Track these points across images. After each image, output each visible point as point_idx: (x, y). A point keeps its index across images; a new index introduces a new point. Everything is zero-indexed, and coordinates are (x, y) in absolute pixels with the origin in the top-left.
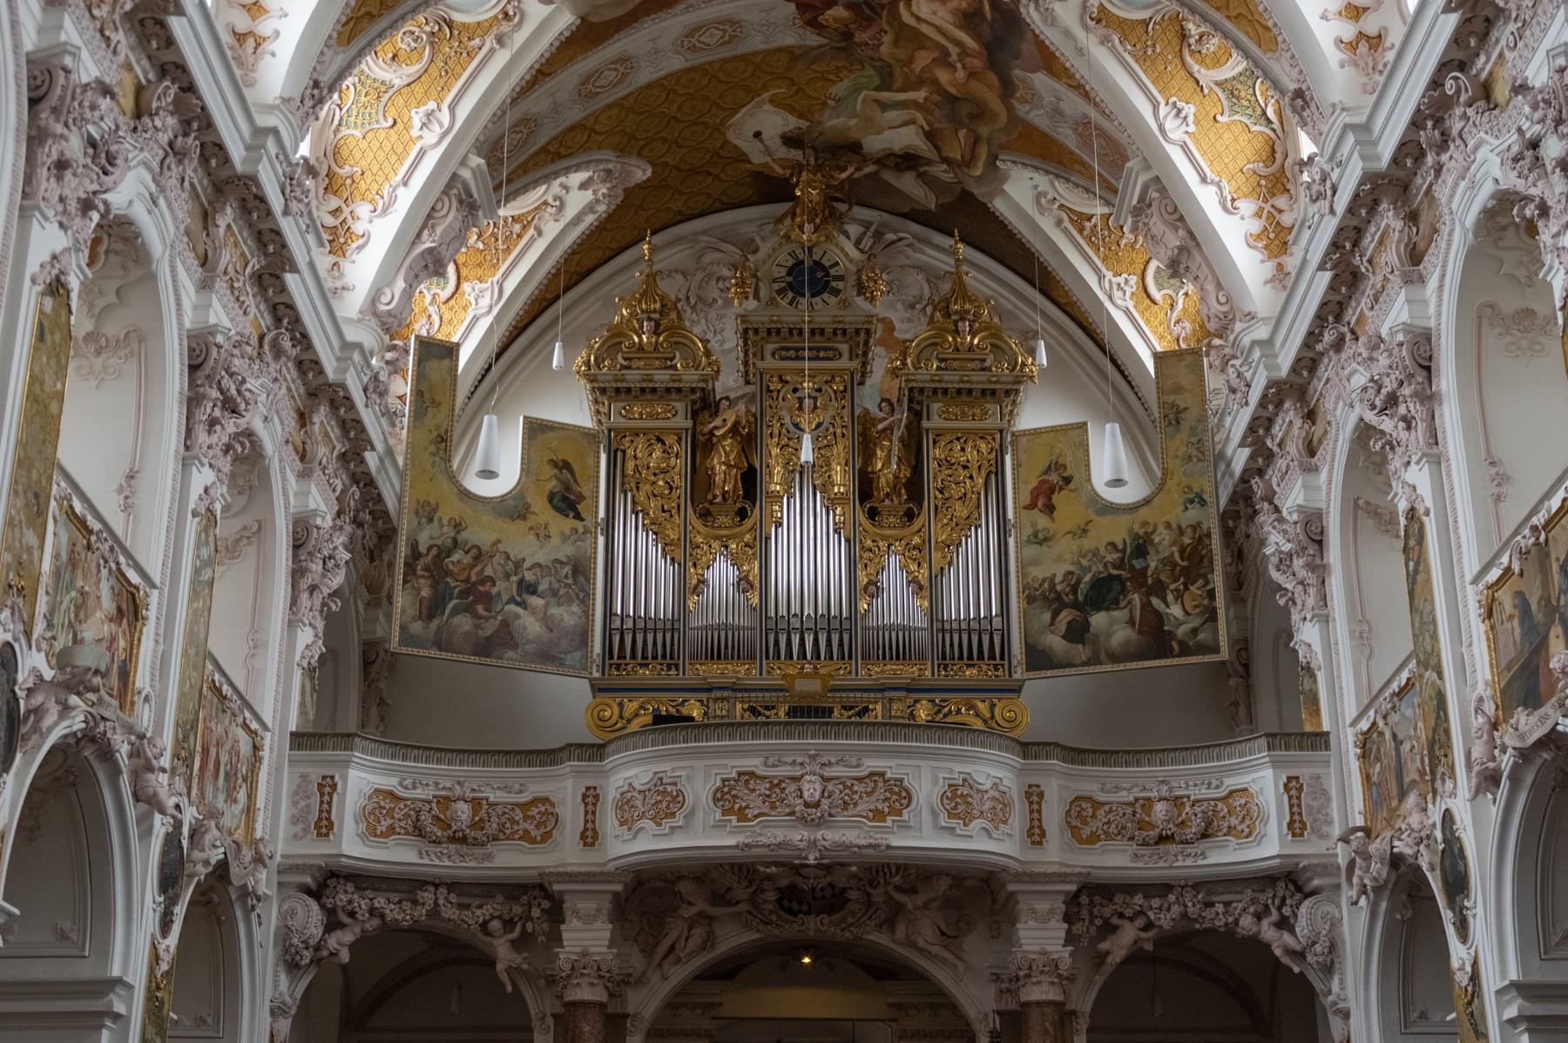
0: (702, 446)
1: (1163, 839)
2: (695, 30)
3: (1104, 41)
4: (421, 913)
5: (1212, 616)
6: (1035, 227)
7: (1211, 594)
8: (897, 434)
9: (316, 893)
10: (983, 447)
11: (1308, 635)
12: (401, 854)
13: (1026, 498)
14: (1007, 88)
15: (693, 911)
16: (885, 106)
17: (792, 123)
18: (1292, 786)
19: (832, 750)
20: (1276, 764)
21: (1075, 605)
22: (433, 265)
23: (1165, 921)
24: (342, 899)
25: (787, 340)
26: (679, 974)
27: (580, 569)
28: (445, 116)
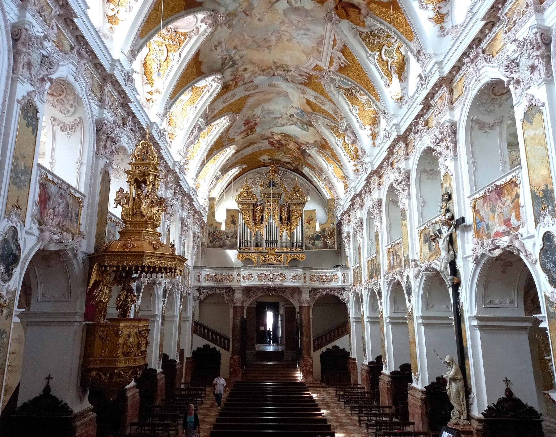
0: (255, 212)
1: (324, 282)
2: (253, 148)
3: (319, 155)
4: (213, 292)
5: (335, 243)
6: (309, 174)
7: (334, 239)
8: (286, 210)
9: (198, 290)
10: (299, 213)
11: (347, 250)
12: (210, 284)
13: (306, 222)
14: (304, 158)
15: (253, 292)
16: (285, 156)
17: (269, 157)
18: (343, 275)
19: (274, 270)
20: (341, 271)
21: (313, 239)
22: (213, 188)
23: (324, 293)
24: (202, 290)
25: (268, 195)
26: (252, 300)
27: (236, 233)
28: (214, 166)
